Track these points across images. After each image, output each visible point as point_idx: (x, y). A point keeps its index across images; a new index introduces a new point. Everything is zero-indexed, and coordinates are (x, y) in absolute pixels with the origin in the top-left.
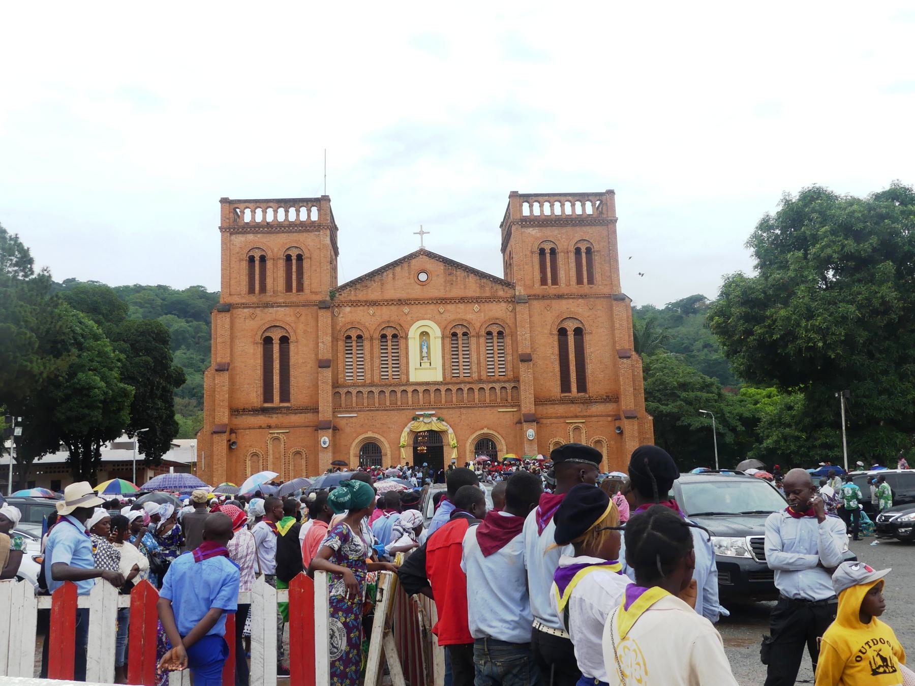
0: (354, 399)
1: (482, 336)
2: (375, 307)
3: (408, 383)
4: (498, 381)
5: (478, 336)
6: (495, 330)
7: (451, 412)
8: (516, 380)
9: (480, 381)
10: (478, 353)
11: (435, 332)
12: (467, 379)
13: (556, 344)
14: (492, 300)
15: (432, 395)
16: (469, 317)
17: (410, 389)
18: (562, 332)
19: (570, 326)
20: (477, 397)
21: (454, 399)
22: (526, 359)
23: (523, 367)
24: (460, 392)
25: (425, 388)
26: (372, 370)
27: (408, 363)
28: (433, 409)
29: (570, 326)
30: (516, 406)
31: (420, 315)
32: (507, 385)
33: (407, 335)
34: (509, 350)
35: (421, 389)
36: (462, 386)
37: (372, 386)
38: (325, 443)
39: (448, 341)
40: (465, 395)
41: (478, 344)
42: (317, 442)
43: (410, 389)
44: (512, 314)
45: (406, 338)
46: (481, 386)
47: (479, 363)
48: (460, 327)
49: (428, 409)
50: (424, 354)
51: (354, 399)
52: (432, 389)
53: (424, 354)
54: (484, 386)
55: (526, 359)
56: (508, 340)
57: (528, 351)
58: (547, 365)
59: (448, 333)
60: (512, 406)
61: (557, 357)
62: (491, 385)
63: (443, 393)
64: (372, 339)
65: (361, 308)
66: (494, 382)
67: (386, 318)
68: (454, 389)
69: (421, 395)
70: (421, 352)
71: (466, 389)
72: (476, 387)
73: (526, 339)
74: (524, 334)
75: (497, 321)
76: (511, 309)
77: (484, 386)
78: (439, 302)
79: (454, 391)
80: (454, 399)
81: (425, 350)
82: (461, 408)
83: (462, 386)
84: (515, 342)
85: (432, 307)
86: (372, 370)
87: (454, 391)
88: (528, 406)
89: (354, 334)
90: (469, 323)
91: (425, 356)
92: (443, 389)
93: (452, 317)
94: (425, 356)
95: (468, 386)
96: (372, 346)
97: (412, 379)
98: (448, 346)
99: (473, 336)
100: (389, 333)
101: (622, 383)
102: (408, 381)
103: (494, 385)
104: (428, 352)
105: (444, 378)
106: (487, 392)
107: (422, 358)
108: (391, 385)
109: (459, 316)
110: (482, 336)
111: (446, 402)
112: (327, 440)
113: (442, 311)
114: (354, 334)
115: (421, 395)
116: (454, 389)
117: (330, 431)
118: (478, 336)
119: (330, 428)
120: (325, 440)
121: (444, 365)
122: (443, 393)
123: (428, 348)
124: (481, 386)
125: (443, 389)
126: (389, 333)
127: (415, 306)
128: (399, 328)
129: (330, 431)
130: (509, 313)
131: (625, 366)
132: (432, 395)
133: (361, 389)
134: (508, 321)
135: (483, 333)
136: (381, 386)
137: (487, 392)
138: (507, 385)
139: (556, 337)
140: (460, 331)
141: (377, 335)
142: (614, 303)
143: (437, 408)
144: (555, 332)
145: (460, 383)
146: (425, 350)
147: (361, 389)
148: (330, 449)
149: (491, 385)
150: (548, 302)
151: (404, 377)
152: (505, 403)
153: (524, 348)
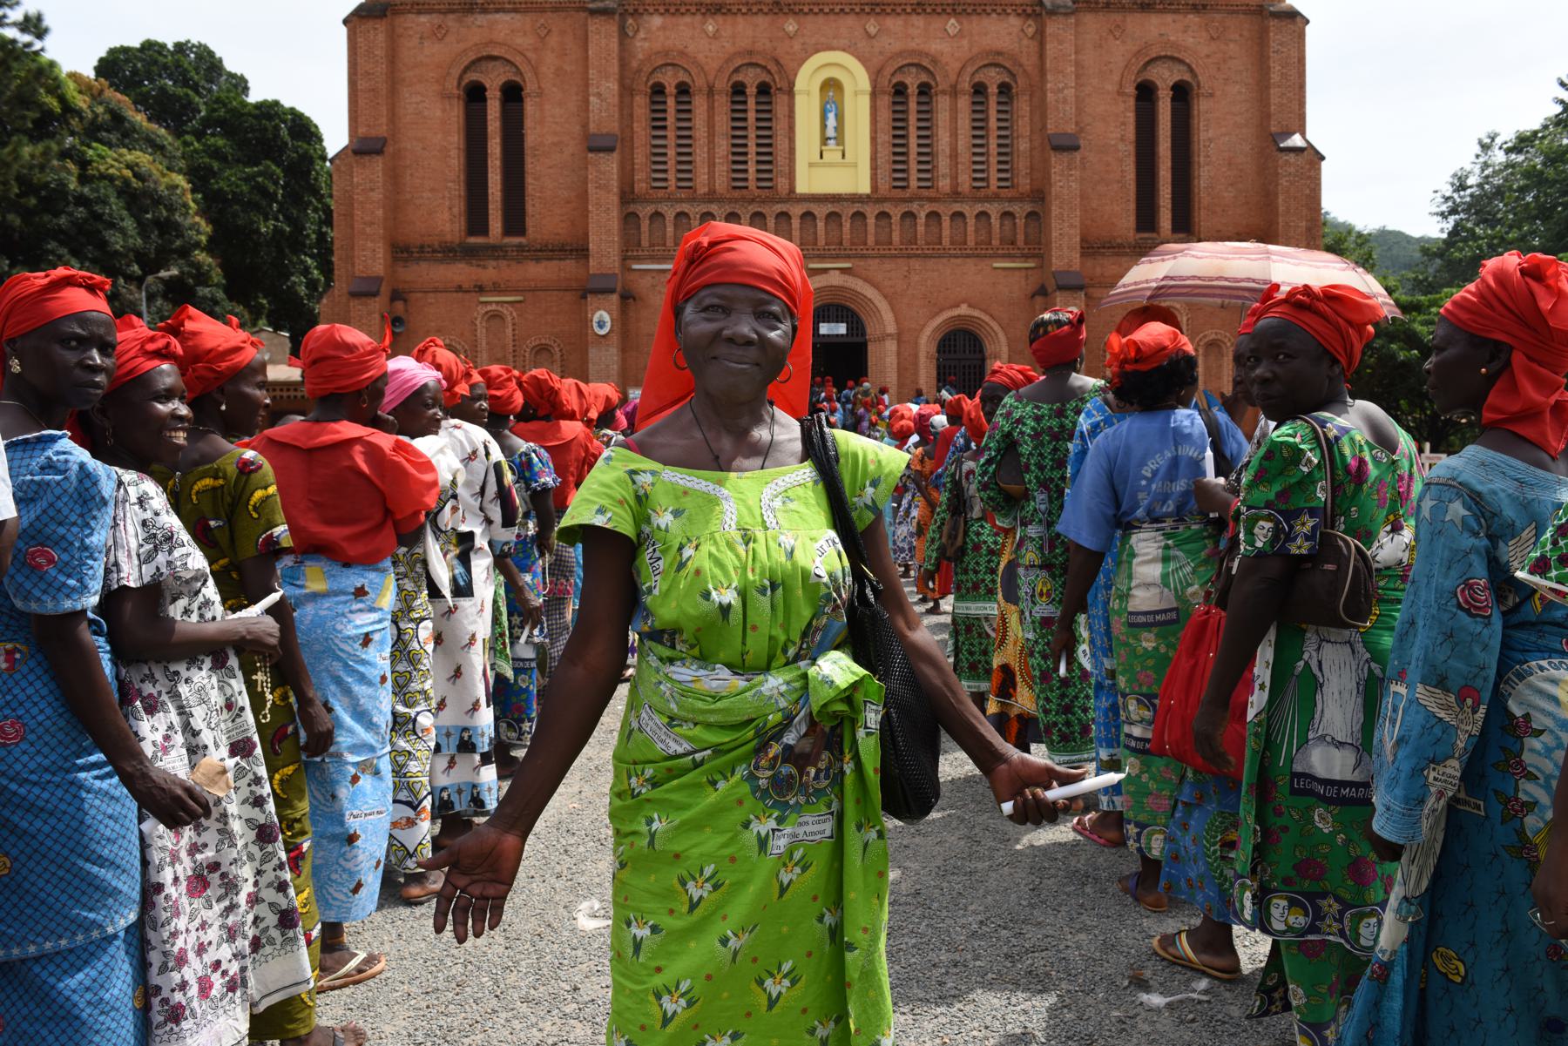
0: (670, 229)
1: (963, 92)
2: (720, 18)
3: (792, 197)
4: (996, 198)
5: (954, 92)
6: (993, 79)
7: (888, 265)
8: (1039, 195)
9: (956, 195)
10: (954, 134)
11: (857, 79)
12: (925, 193)
13: (1131, 117)
14: (989, 9)
15: (847, 225)
16: (936, 46)
17: (796, 211)
18: (1146, 92)
19: (1164, 78)
20: (946, 232)
21: (896, 237)
22: (1066, 146)
23: (1057, 163)
24: (908, 221)
25: (830, 208)
26: (712, 165)
27: (792, 151)
28: (848, 257)
29: (1164, 78)
30: (1034, 256)
31: (823, 40)
32: (1015, 208)
33: (792, 85)
34: (1023, 126)
35: (821, 211)
36: (914, 207)
37: (711, 201)
38: (601, 324)
39: (885, 101)
40: (921, 229)
41: (954, 111)
42: (586, 323)
43: (796, 211)
44: (1034, 45)
45: (790, 93)
46: (957, 207)
47: (954, 155)
48: (914, 70)
49: (837, 258)
50: (831, 132)
51: (670, 229)
52: (848, 211)
53: (831, 132)
54: (965, 208)
55: (1066, 146)
56: (1023, 106)
57: (1071, 128)
58: (1108, 164)
59: (884, 82)
60: (1026, 257)
61: (1132, 148)
62: (979, 208)
63: (871, 221)
64: (711, 92)
65: (687, 19)
66: (987, 199)
67: (744, 43)
68: (896, 212)
69: (821, 225)
70: (824, 126)
71: (923, 215)
72: (946, 210)
73: (1065, 101)
74: (1061, 89)
75: (1000, 60)
76: (1031, 31)
77: (965, 208)
78: (867, 9)
79: (896, 219)
80: (896, 237)
81: (831, 121)
82: (909, 257)
83: (914, 207)
84: (1040, 109)
85: (850, 20)
86: (712, 165)
87: (896, 219)
88: (1065, 253)
89: (670, 80)
90: (934, 61)
91: (831, 137)
92: (871, 212)
93: (897, 46)
94: (831, 137)
95: (928, 208)
96: (711, 109)
97: (802, 187)
98: (885, 115)
99: (944, 92)
100: (751, 79)
101: (1281, 209)
102: (792, 189)
103: (987, 207)
104: (840, 128)
105: (874, 187)
106: (971, 222)
107: (825, 140)
108: (752, 201)
109: (913, 45)
110: (963, 92)
111: (877, 243)
112: (607, 318)
113: (872, 30)
114: (670, 80)
115: (821, 225)
116: (896, 212)
117: (615, 298)
118: (954, 92)
119: (612, 291)
120: (602, 318)
121: (874, 159)
122: (871, 221)
123: (840, 118)
124: (957, 207)
125: (871, 212)
126: (751, 79)
127: (810, 18)
128: (772, 67)
129: (615, 298)
130: (1025, 42)
131: (1292, 170)
132: (847, 225)
133: (685, 207)
134: (1024, 60)
135: (966, 85)
136: (731, 200)
137: (971, 222)
138: (1015, 208)
139: (1132, 102)
140: (912, 81)
141: (723, 84)
142: (1273, 23)
143: (855, 256)
144: (1131, 90)
145: (910, 200)
146: (831, 121)
147: (685, 207)
148: (615, 338)
149: (979, 208)
150: (1117, 17)
151: (782, 184)
152: (1009, 246)
153: (1060, 121)
